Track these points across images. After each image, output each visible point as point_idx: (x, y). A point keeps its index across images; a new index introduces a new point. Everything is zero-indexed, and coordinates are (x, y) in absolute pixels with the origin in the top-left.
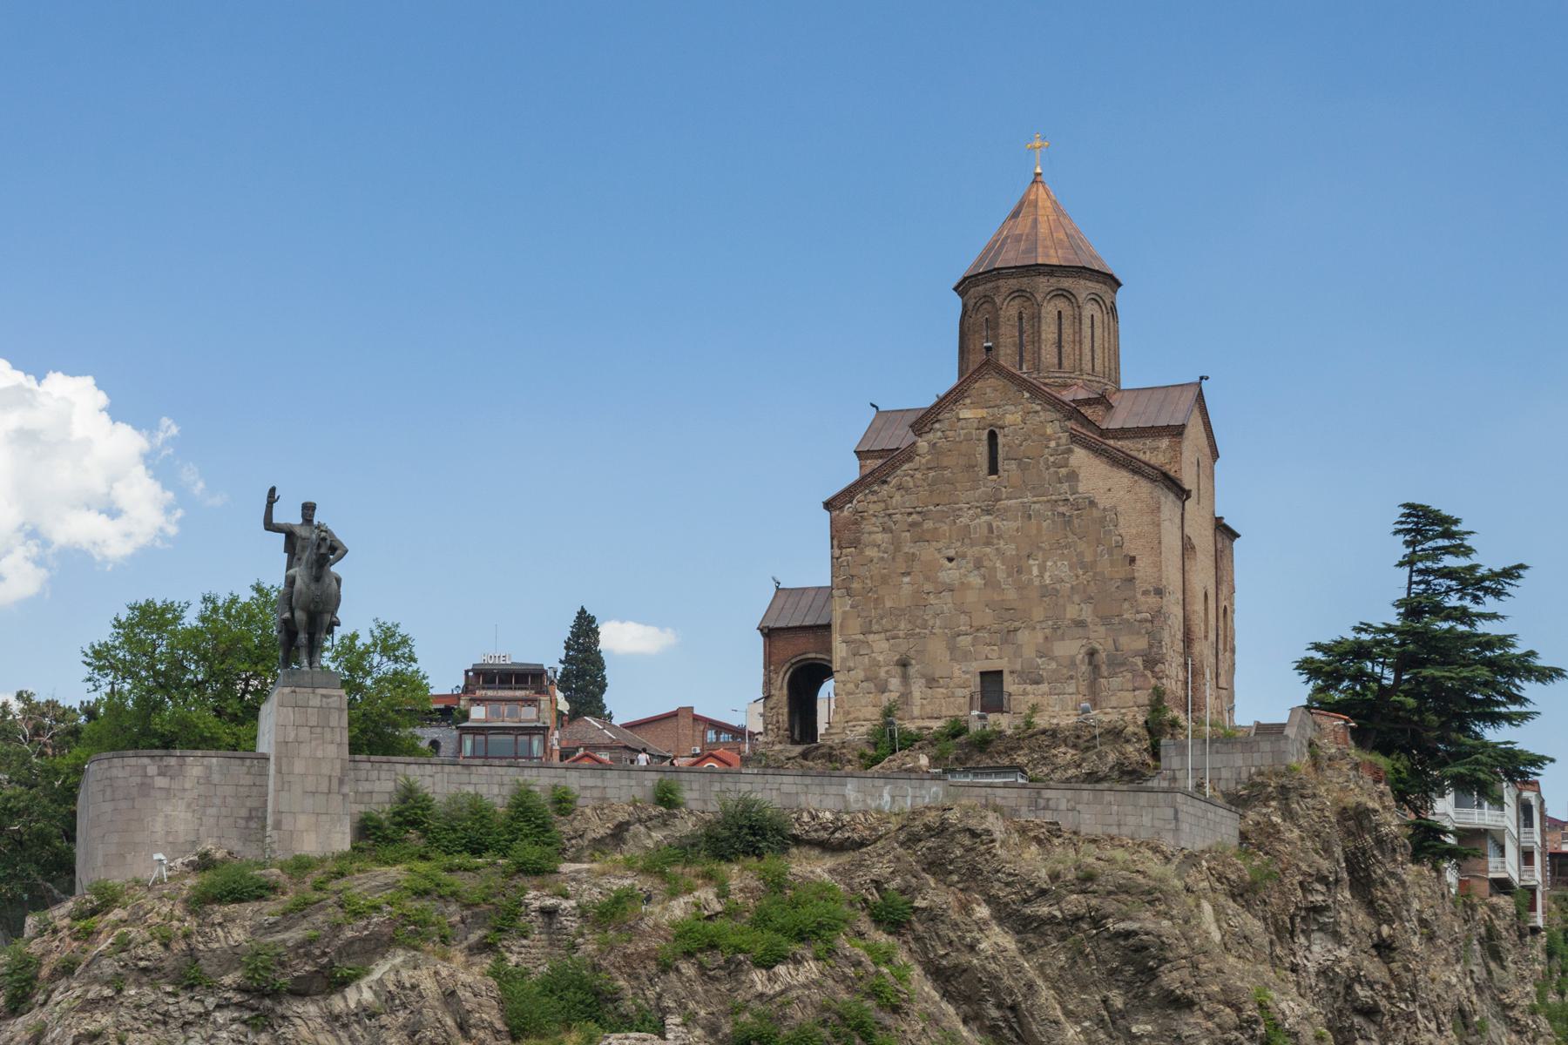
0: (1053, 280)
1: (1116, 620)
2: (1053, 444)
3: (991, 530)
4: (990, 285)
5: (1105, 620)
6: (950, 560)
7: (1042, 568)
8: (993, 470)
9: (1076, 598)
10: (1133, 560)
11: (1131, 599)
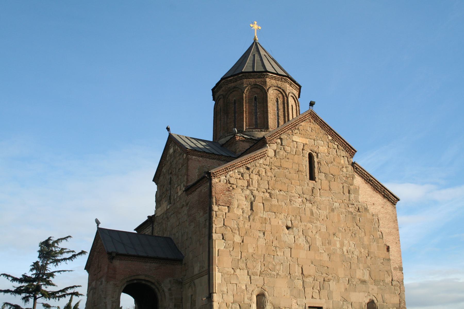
0: (291, 88)
1: (382, 284)
2: (344, 170)
3: (312, 213)
4: (260, 80)
5: (376, 282)
6: (288, 228)
7: (342, 245)
8: (312, 177)
9: (361, 265)
10: (388, 248)
11: (389, 272)
